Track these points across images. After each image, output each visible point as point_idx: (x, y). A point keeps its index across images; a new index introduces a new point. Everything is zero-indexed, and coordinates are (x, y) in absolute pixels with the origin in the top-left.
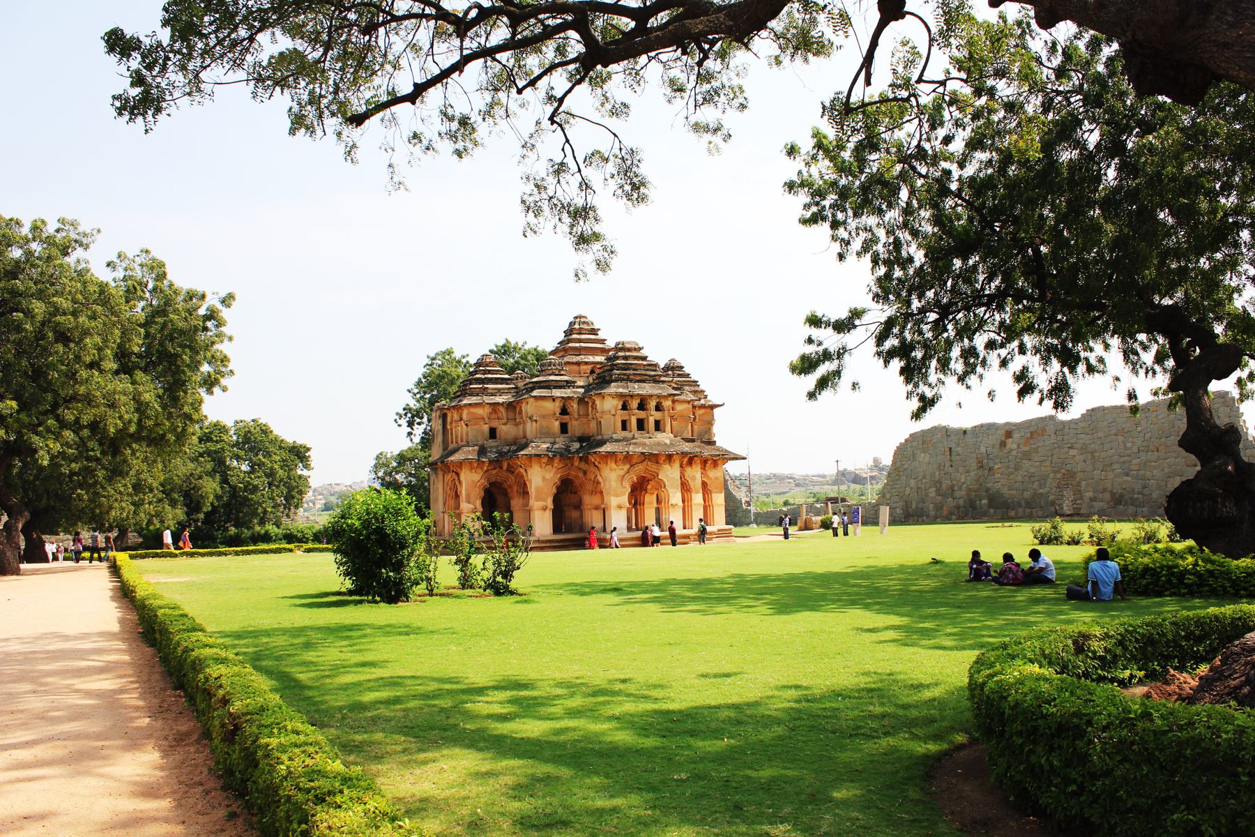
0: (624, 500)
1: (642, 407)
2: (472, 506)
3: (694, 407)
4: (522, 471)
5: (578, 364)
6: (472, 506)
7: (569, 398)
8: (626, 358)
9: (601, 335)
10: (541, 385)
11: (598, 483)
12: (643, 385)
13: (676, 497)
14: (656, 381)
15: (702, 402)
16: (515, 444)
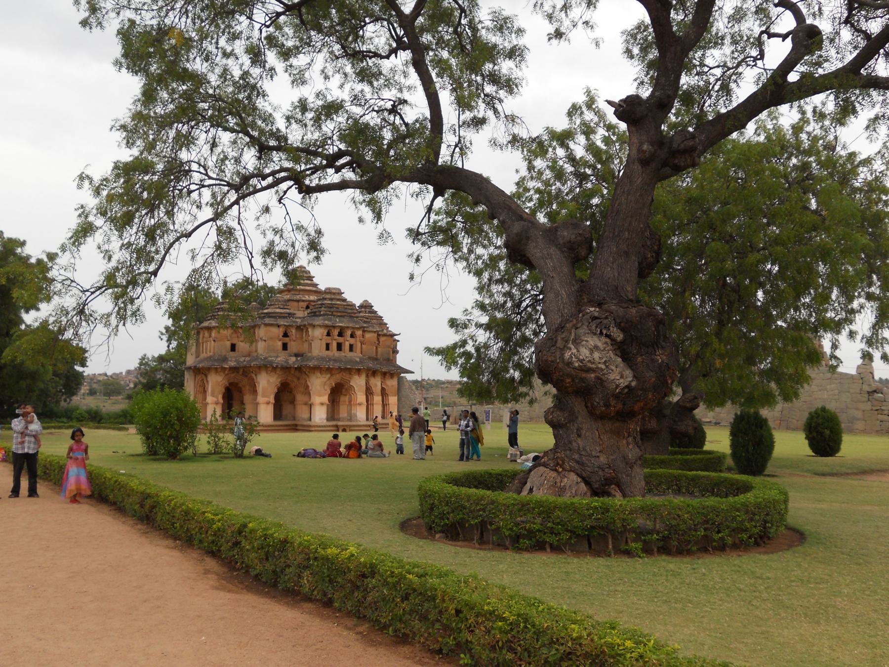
0: (325, 399)
1: (340, 334)
2: (215, 399)
3: (379, 335)
4: (254, 376)
5: (298, 301)
6: (215, 399)
7: (289, 326)
8: (331, 299)
9: (315, 280)
10: (269, 315)
11: (308, 387)
12: (342, 319)
13: (361, 398)
14: (351, 317)
15: (385, 331)
16: (249, 355)
